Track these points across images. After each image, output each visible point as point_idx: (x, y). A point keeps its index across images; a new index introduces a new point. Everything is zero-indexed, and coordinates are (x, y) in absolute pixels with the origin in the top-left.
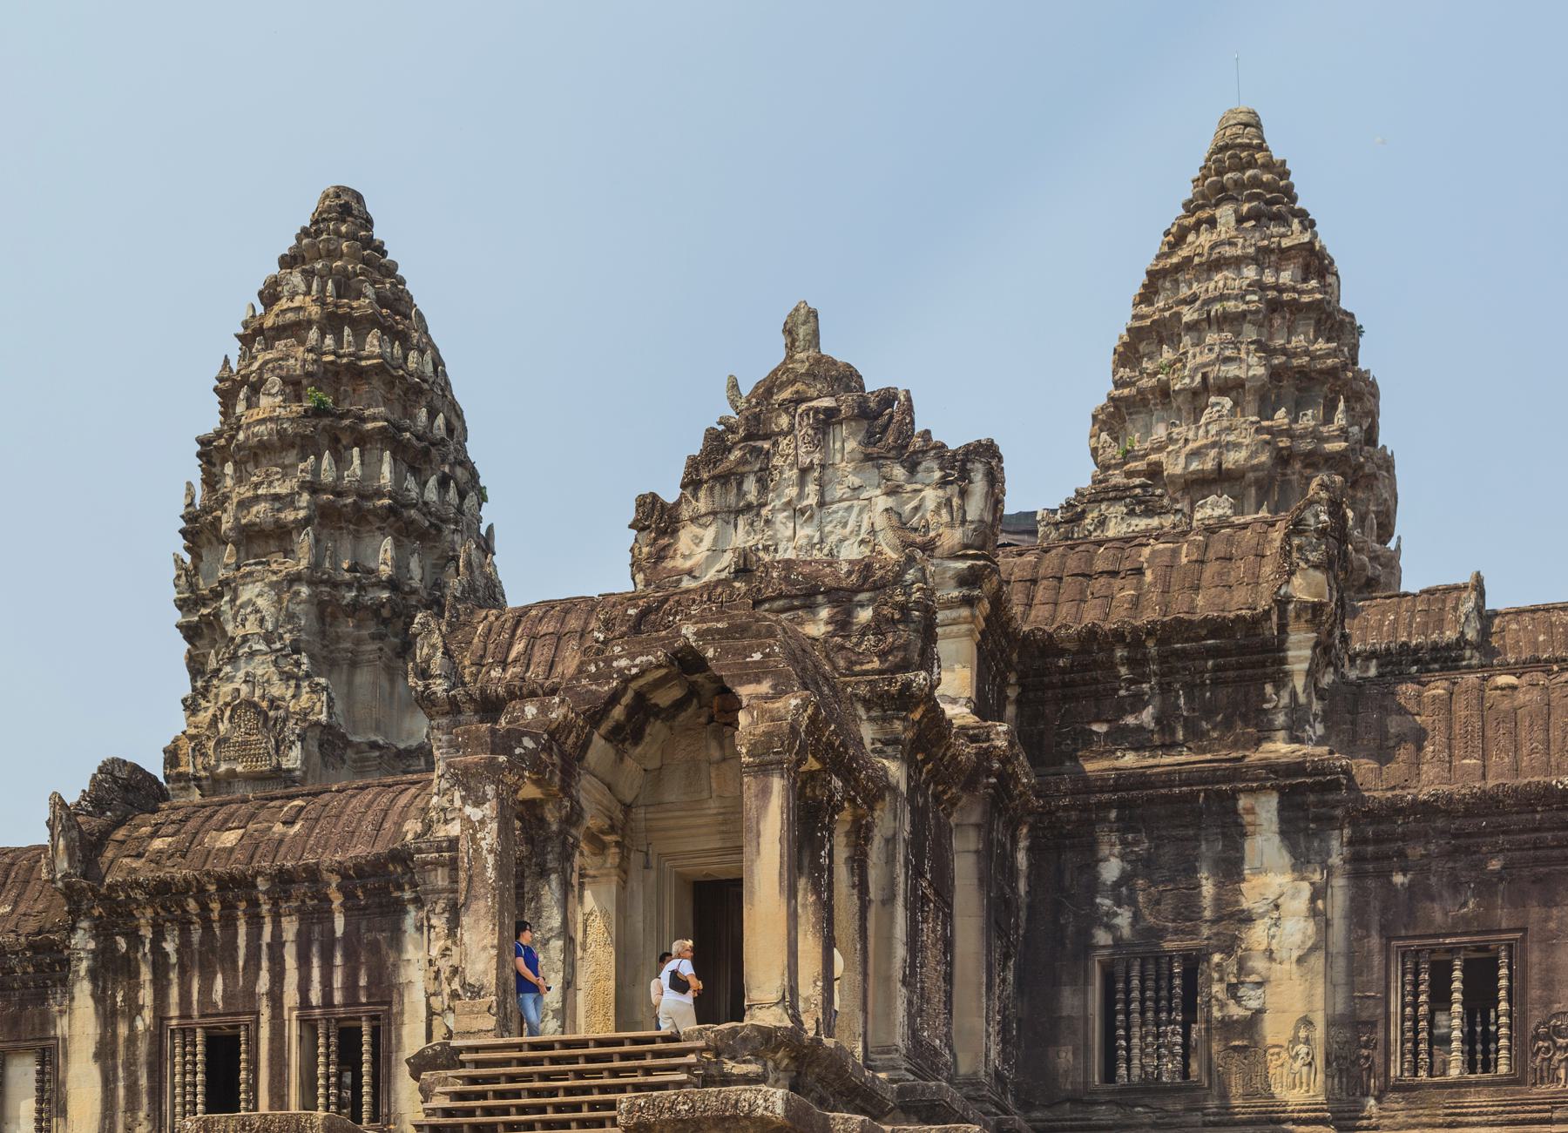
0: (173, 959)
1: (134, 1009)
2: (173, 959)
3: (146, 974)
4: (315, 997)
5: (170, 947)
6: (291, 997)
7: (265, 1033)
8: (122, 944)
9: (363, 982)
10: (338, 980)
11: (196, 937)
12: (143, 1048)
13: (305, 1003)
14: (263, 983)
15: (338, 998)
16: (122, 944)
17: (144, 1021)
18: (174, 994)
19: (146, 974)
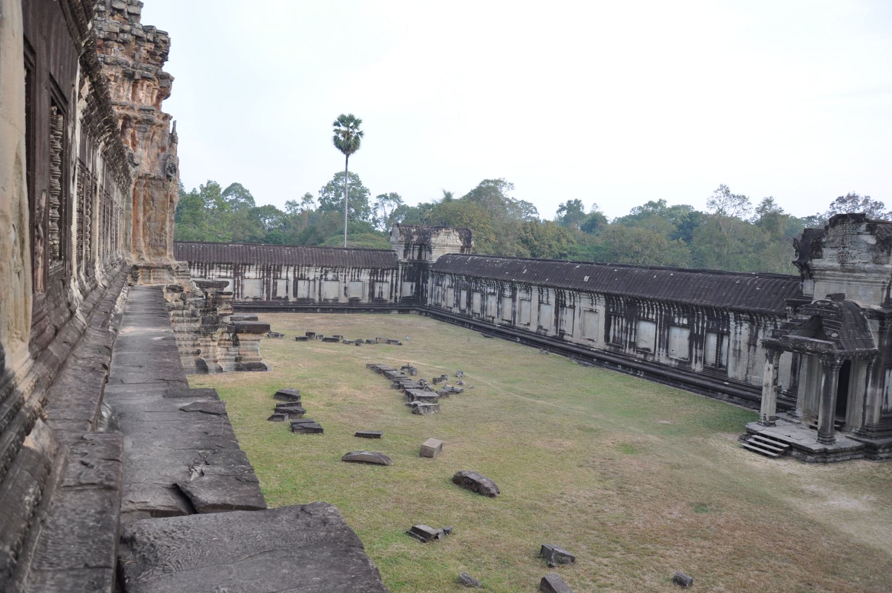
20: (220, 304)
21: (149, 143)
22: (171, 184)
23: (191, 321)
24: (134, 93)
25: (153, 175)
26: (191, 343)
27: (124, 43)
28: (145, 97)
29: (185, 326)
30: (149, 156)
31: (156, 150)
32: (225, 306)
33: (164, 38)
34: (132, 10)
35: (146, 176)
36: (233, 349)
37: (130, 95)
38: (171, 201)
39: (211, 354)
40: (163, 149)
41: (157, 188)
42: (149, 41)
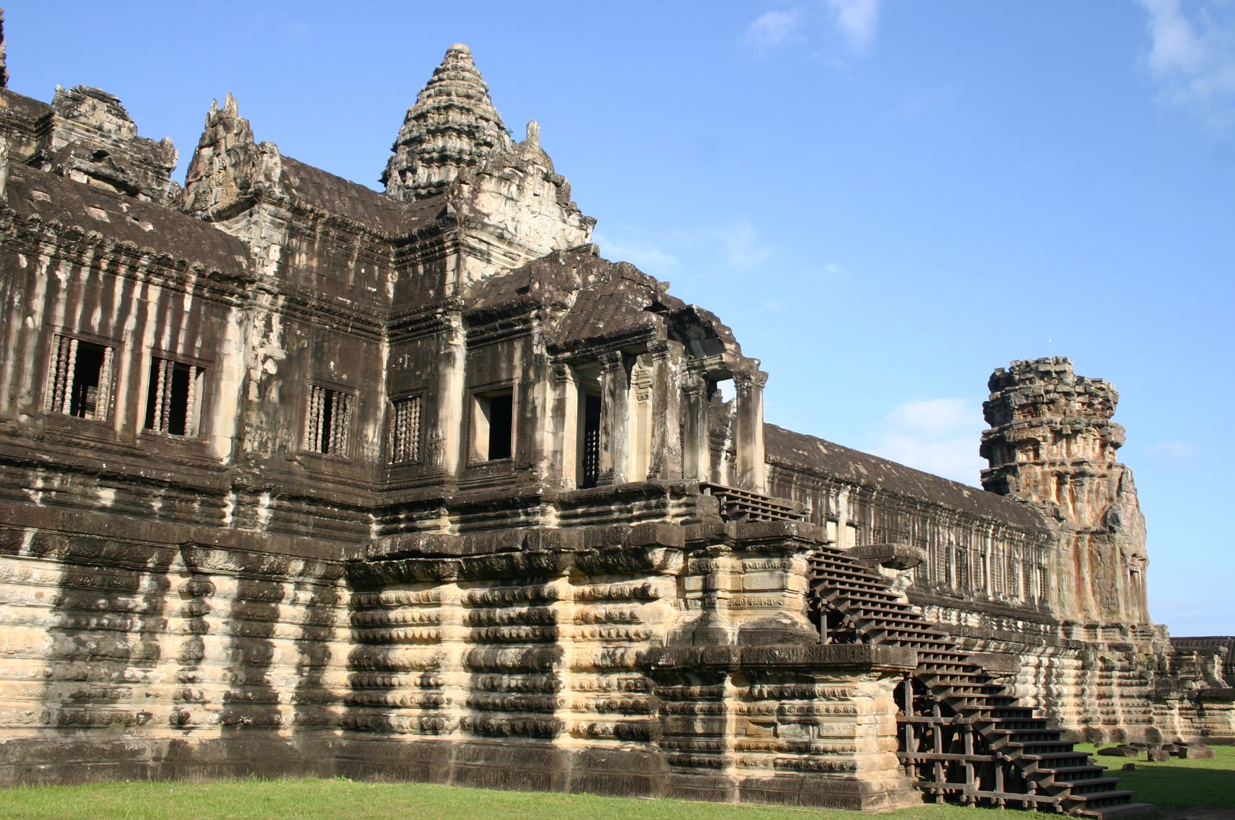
0: (64, 285)
1: (29, 312)
2: (64, 285)
3: (41, 288)
4: (165, 343)
5: (62, 275)
6: (148, 339)
7: (127, 358)
8: (24, 262)
9: (198, 344)
10: (182, 338)
11: (85, 274)
12: (32, 342)
13: (156, 348)
14: (131, 323)
15: (180, 350)
16: (24, 262)
17: (34, 322)
18: (60, 310)
19: (41, 288)
20: (1180, 666)
21: (1093, 496)
22: (1117, 536)
23: (1141, 685)
24: (1068, 449)
25: (1093, 529)
26: (1143, 709)
27: (1052, 402)
28: (1085, 448)
29: (1134, 690)
30: (1093, 509)
31: (1103, 503)
32: (1186, 669)
33: (1099, 385)
34: (1058, 368)
35: (1086, 530)
36: (1197, 720)
37: (1064, 451)
38: (1122, 554)
39: (1168, 724)
40: (1111, 499)
41: (1104, 541)
42: (1079, 394)
